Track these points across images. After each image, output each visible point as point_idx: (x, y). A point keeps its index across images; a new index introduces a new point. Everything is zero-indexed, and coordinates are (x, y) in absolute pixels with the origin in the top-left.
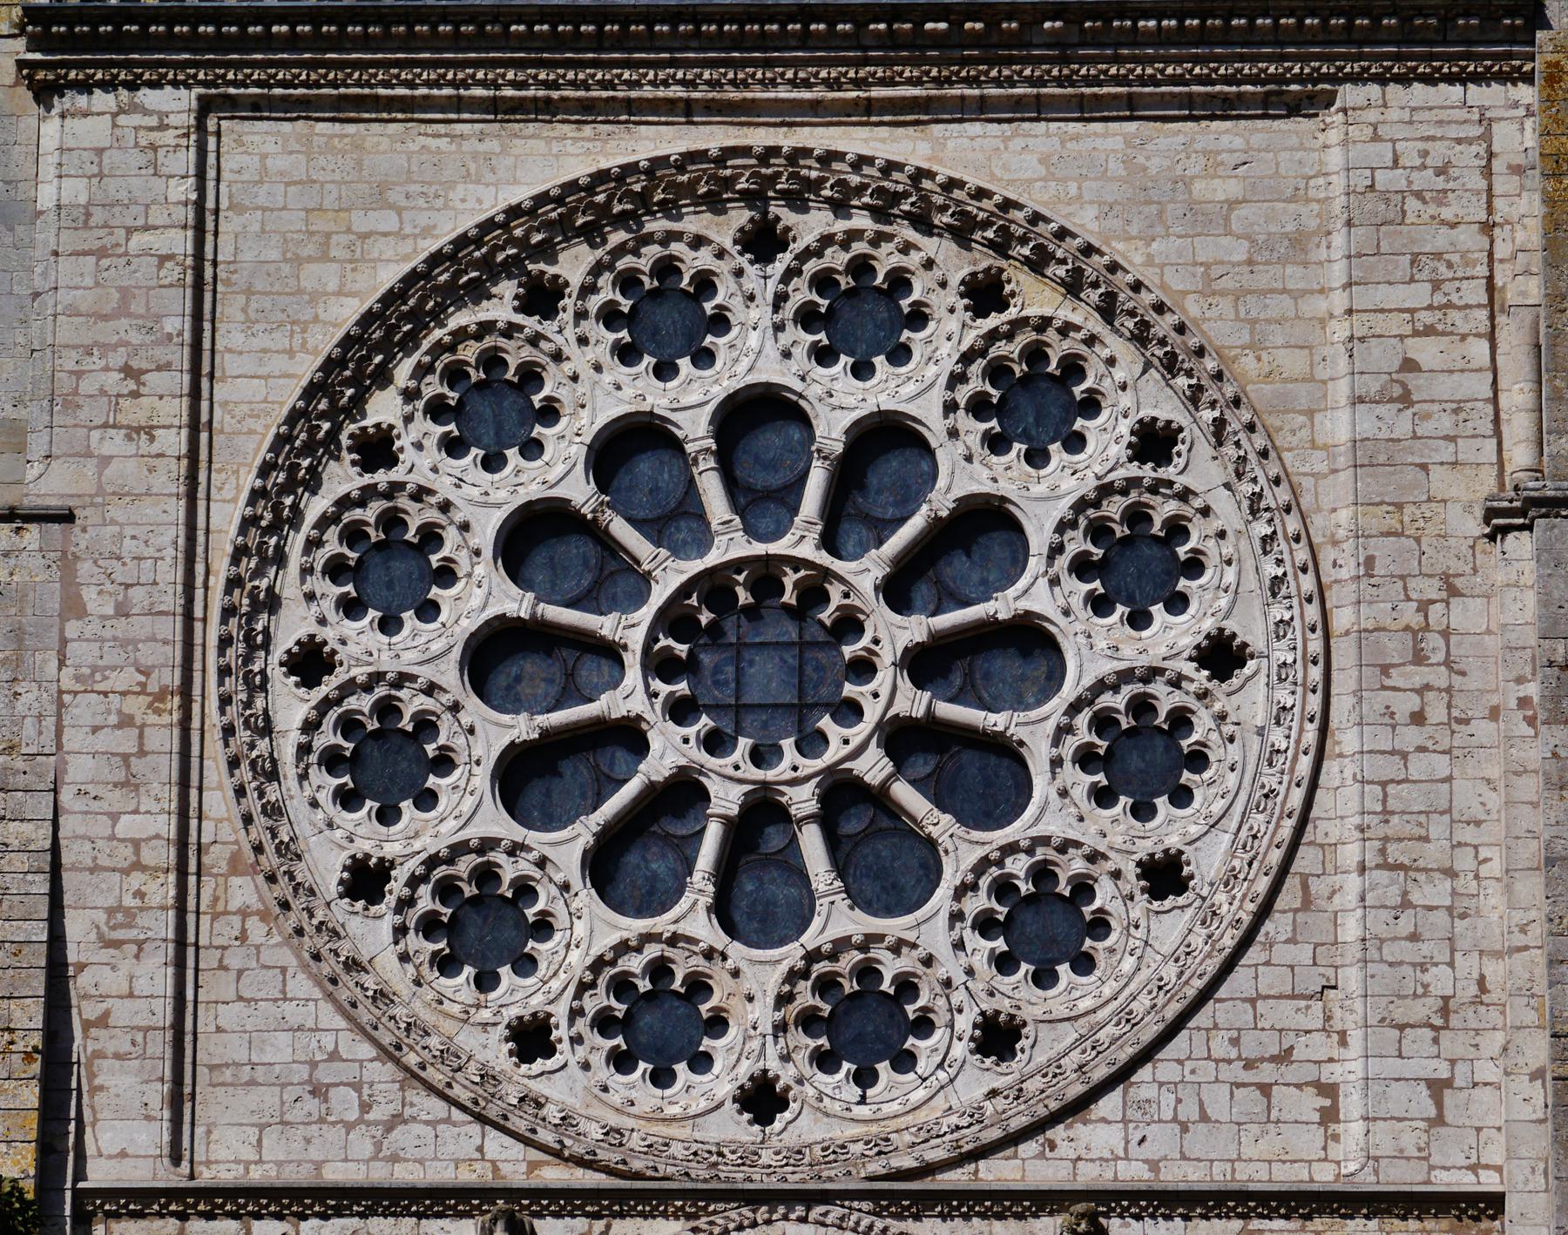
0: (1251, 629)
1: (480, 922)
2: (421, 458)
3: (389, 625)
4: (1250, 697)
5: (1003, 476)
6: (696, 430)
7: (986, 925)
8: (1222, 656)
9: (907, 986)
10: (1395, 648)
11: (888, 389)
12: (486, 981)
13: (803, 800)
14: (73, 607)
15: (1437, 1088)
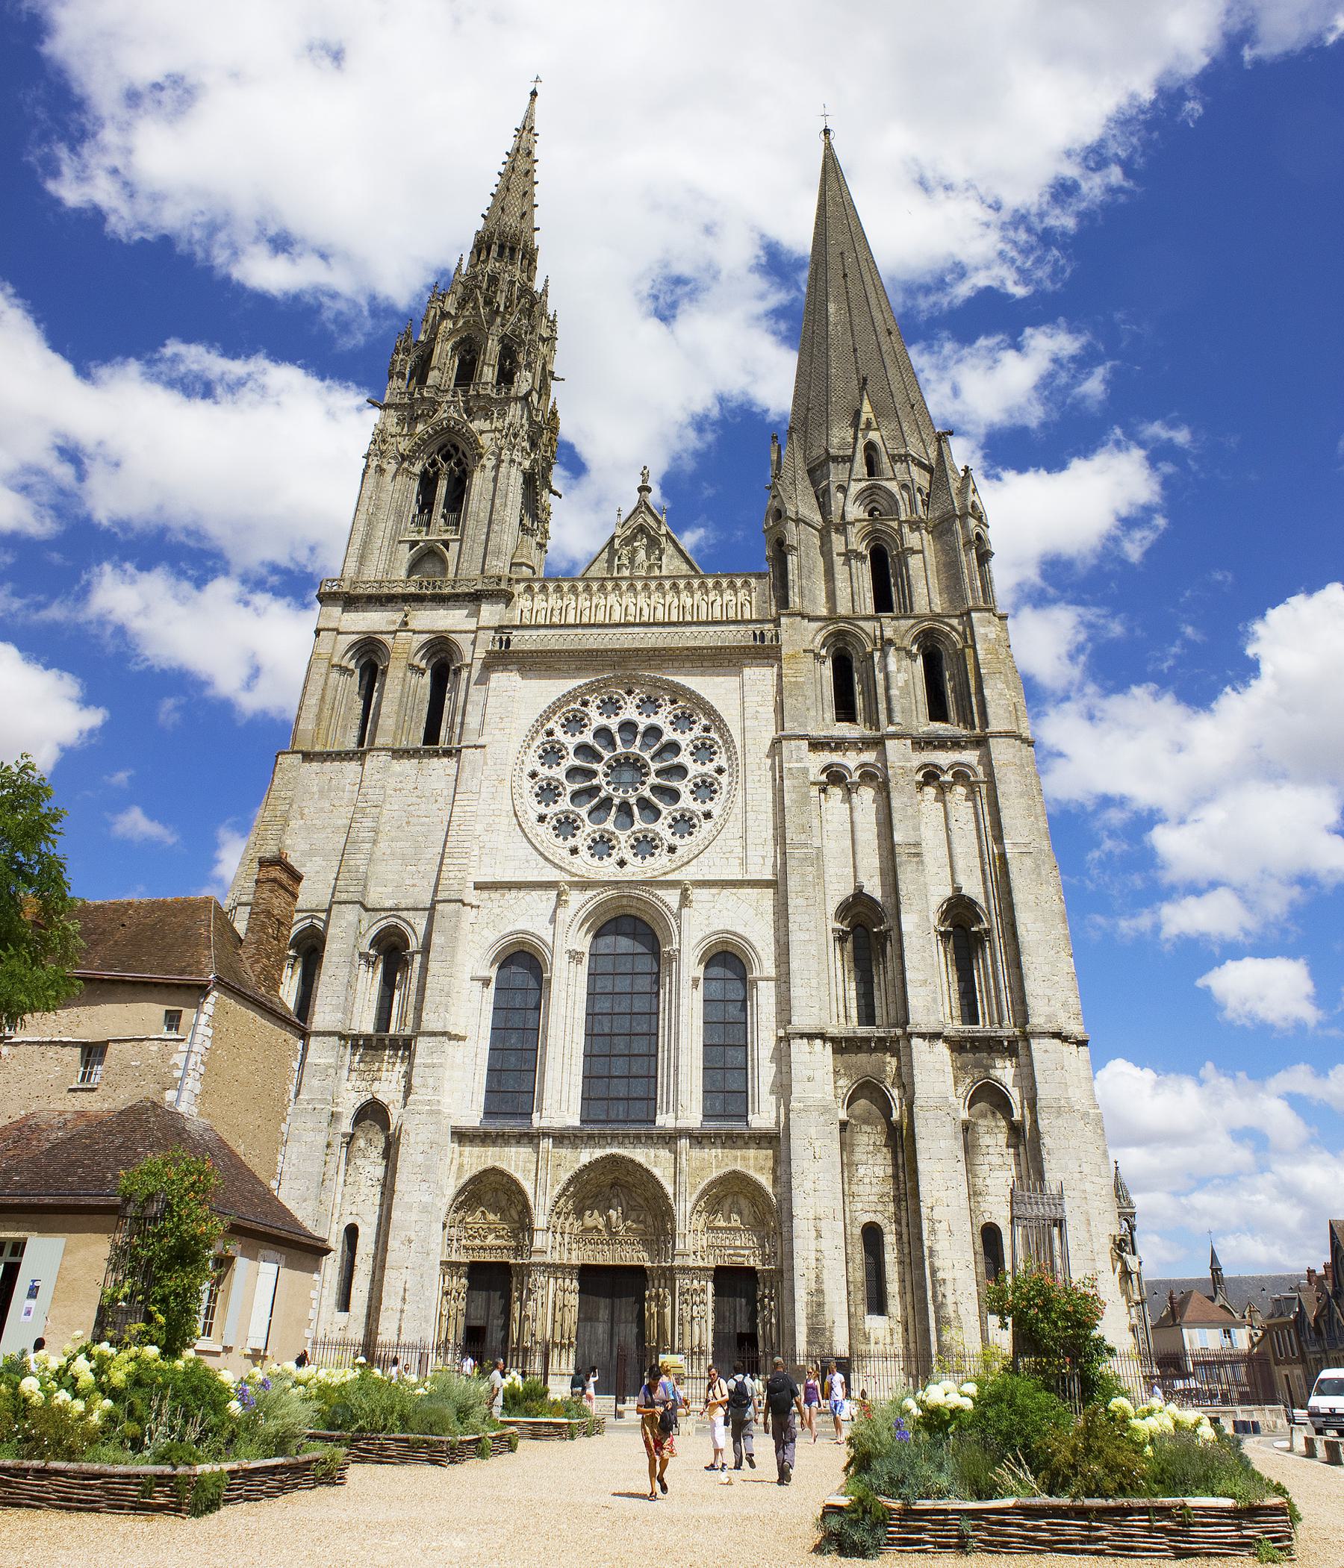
0: (725, 766)
1: (566, 826)
2: (559, 734)
3: (550, 767)
4: (724, 779)
5: (677, 736)
6: (614, 728)
7: (670, 827)
8: (720, 771)
9: (653, 840)
10: (755, 767)
11: (654, 720)
12: (565, 839)
13: (633, 801)
14: (485, 763)
15: (763, 857)
